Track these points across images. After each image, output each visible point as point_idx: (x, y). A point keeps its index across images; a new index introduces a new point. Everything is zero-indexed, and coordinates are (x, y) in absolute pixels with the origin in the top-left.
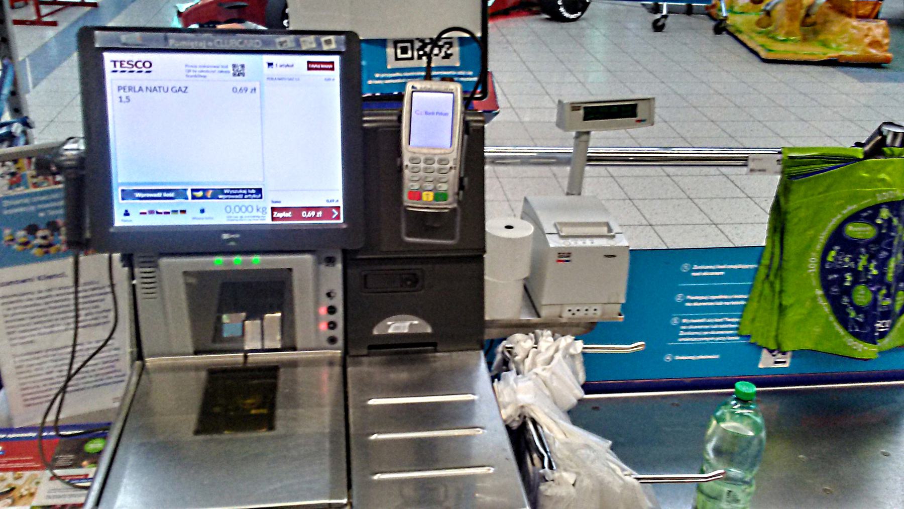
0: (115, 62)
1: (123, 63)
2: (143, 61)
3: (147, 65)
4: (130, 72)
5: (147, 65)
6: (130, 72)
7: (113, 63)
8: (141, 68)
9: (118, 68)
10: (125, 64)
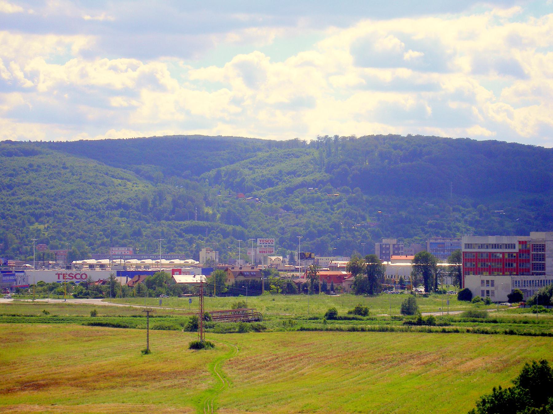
0: (59, 274)
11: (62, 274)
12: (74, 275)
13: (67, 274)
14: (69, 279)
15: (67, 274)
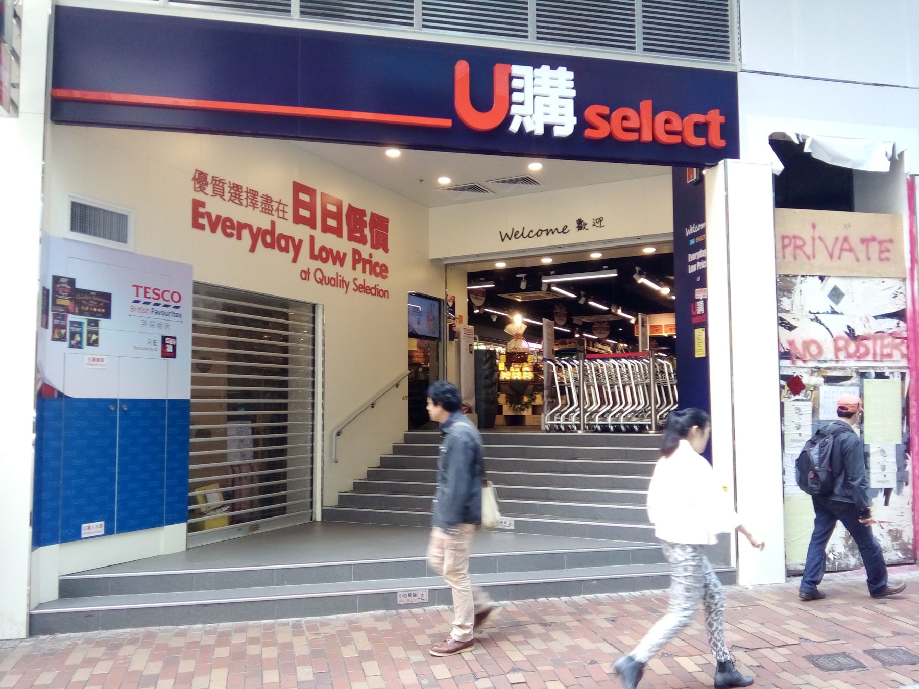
0: (138, 287)
1: (148, 290)
2: (171, 292)
3: (176, 297)
5: (176, 297)
7: (135, 288)
9: (141, 298)
11: (141, 287)
12: (162, 291)
13: (149, 288)
15: (149, 288)
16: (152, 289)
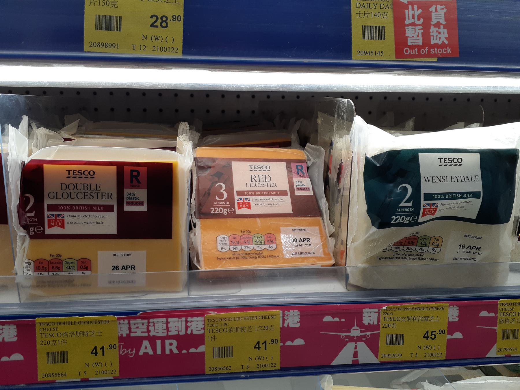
0: (441, 159)
1: (446, 159)
4: (450, 165)
5: (460, 160)
6: (450, 165)
8: (456, 163)
9: (443, 163)
10: (447, 161)
11: (443, 159)
12: (452, 159)
13: (447, 159)
14: (449, 163)
15: (447, 159)
16: (448, 159)
